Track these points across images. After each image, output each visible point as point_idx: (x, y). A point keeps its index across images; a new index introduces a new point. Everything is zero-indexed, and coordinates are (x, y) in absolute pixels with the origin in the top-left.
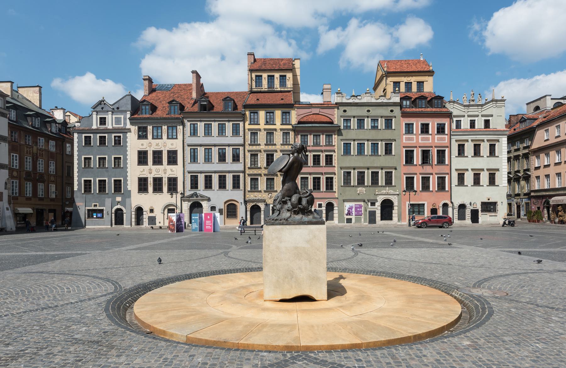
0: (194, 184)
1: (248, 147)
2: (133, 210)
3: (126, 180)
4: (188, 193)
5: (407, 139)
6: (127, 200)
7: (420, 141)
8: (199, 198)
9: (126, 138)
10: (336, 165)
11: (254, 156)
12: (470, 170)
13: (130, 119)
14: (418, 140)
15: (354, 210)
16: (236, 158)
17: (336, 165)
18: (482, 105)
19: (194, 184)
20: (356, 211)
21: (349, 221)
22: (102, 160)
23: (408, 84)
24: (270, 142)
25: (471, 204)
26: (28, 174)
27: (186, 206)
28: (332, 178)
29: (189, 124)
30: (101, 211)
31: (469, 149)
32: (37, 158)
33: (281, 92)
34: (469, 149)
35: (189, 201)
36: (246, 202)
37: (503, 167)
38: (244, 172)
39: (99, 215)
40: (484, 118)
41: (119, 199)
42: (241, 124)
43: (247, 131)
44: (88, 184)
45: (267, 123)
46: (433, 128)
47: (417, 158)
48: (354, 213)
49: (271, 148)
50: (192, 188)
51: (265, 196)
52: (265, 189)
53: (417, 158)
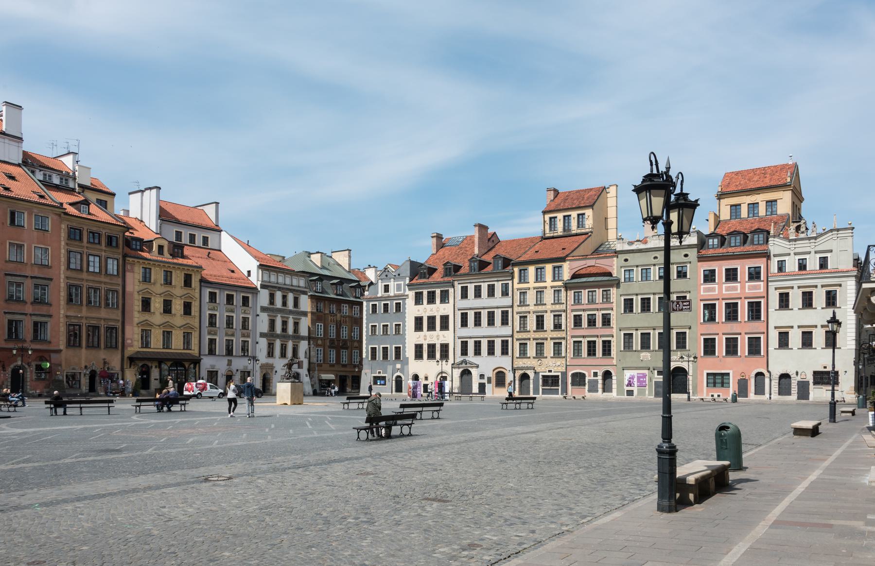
0: (464, 352)
1: (516, 309)
2: (411, 377)
3: (404, 347)
4: (459, 358)
5: (727, 289)
6: (406, 367)
7: (724, 292)
8: (468, 365)
9: (405, 304)
10: (615, 326)
11: (523, 318)
12: (796, 327)
13: (408, 285)
14: (721, 290)
15: (635, 380)
16: (505, 322)
17: (615, 326)
18: (815, 238)
19: (464, 352)
20: (639, 381)
21: (630, 393)
22: (385, 326)
23: (753, 206)
24: (539, 302)
25: (797, 373)
26: (332, 341)
27: (457, 373)
28: (609, 342)
29: (460, 286)
30: (384, 378)
31: (796, 299)
32: (340, 325)
33: (576, 235)
34: (796, 299)
35: (459, 368)
36: (514, 370)
37: (849, 322)
38: (512, 336)
39: (382, 382)
40: (819, 256)
41: (398, 366)
42: (510, 282)
43: (515, 291)
44: (374, 350)
45: (537, 281)
46: (743, 273)
47: (721, 313)
48: (636, 383)
49: (540, 308)
50: (462, 354)
51: (534, 363)
52: (552, 355)
53: (721, 313)
